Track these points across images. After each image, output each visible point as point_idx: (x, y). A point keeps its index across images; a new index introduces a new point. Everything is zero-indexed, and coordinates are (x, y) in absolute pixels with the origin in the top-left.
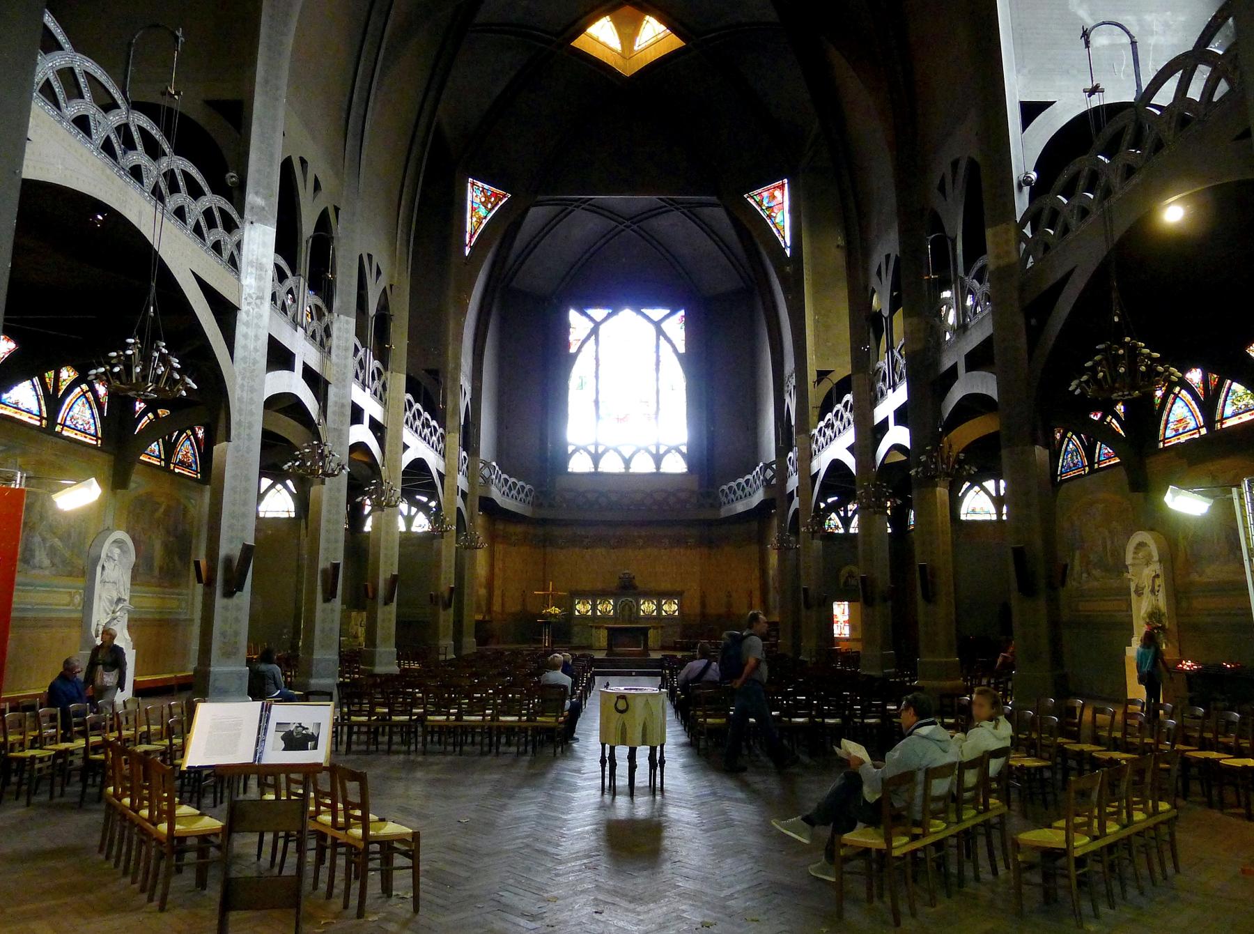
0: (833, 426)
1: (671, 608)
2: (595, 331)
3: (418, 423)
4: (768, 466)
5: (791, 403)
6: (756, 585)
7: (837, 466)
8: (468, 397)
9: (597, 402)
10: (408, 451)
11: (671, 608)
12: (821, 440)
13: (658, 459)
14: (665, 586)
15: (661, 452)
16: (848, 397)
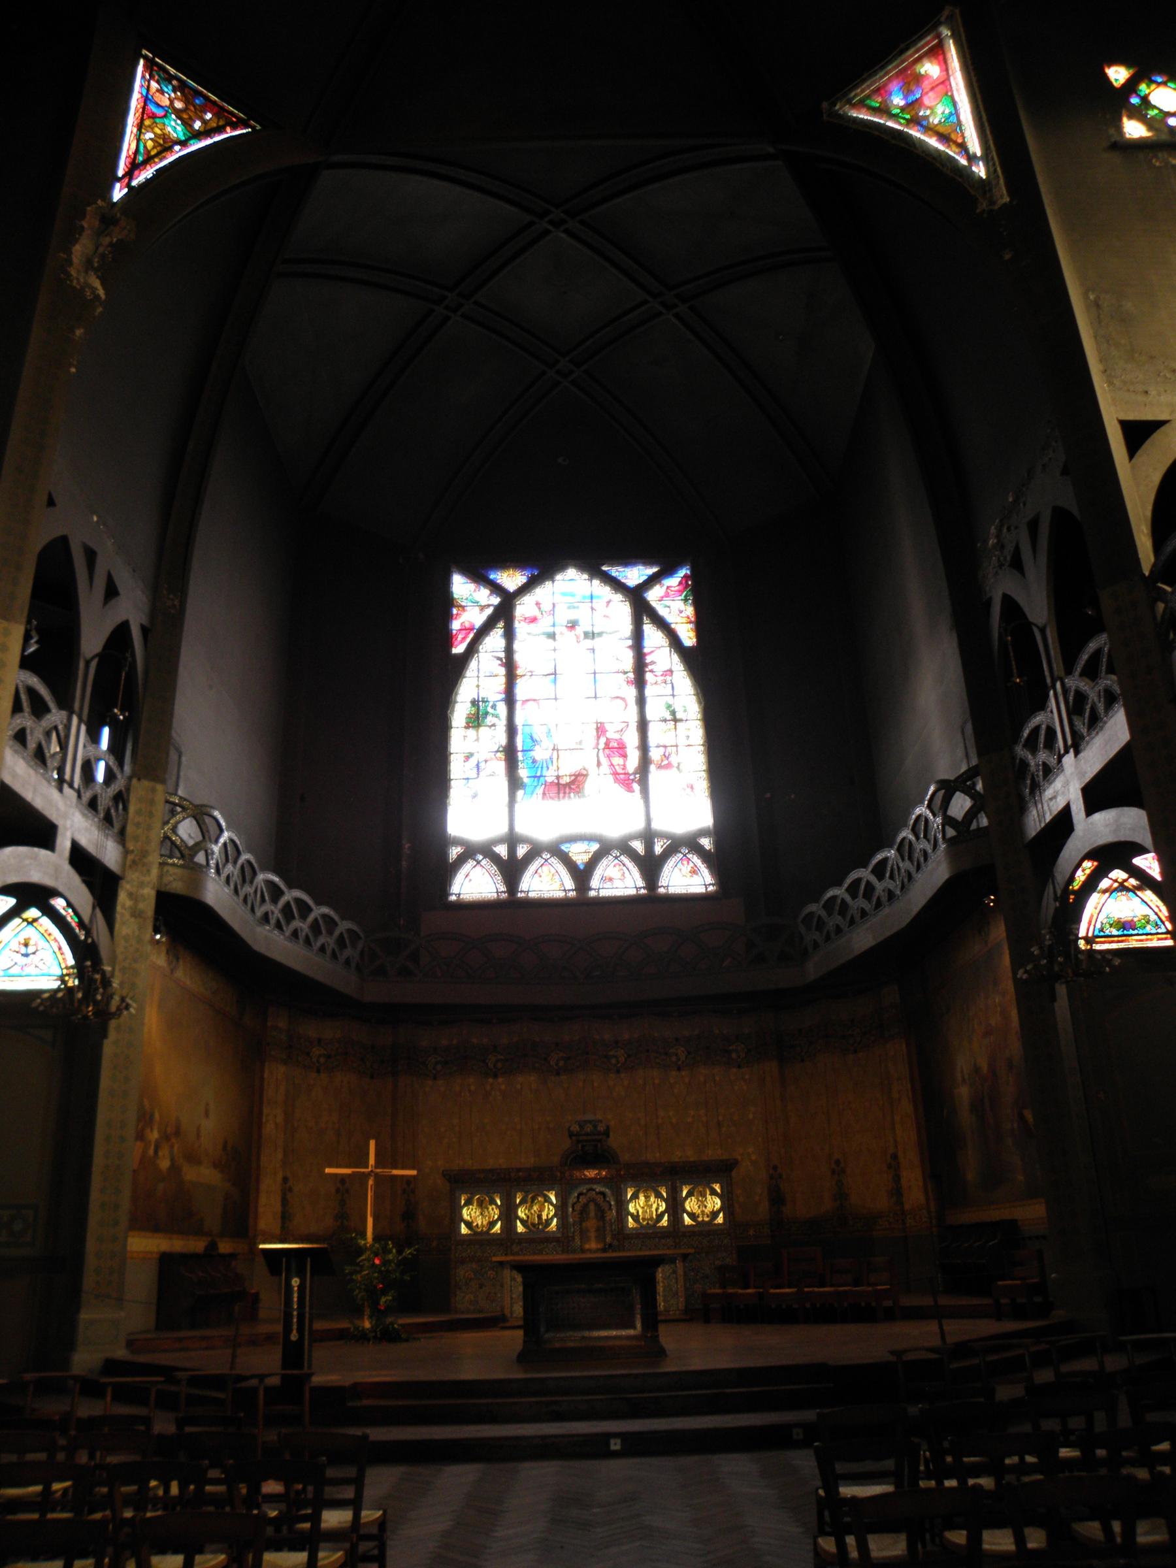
1: (704, 1205)
11: (704, 1205)
13: (650, 866)
14: (684, 1153)
15: (658, 850)
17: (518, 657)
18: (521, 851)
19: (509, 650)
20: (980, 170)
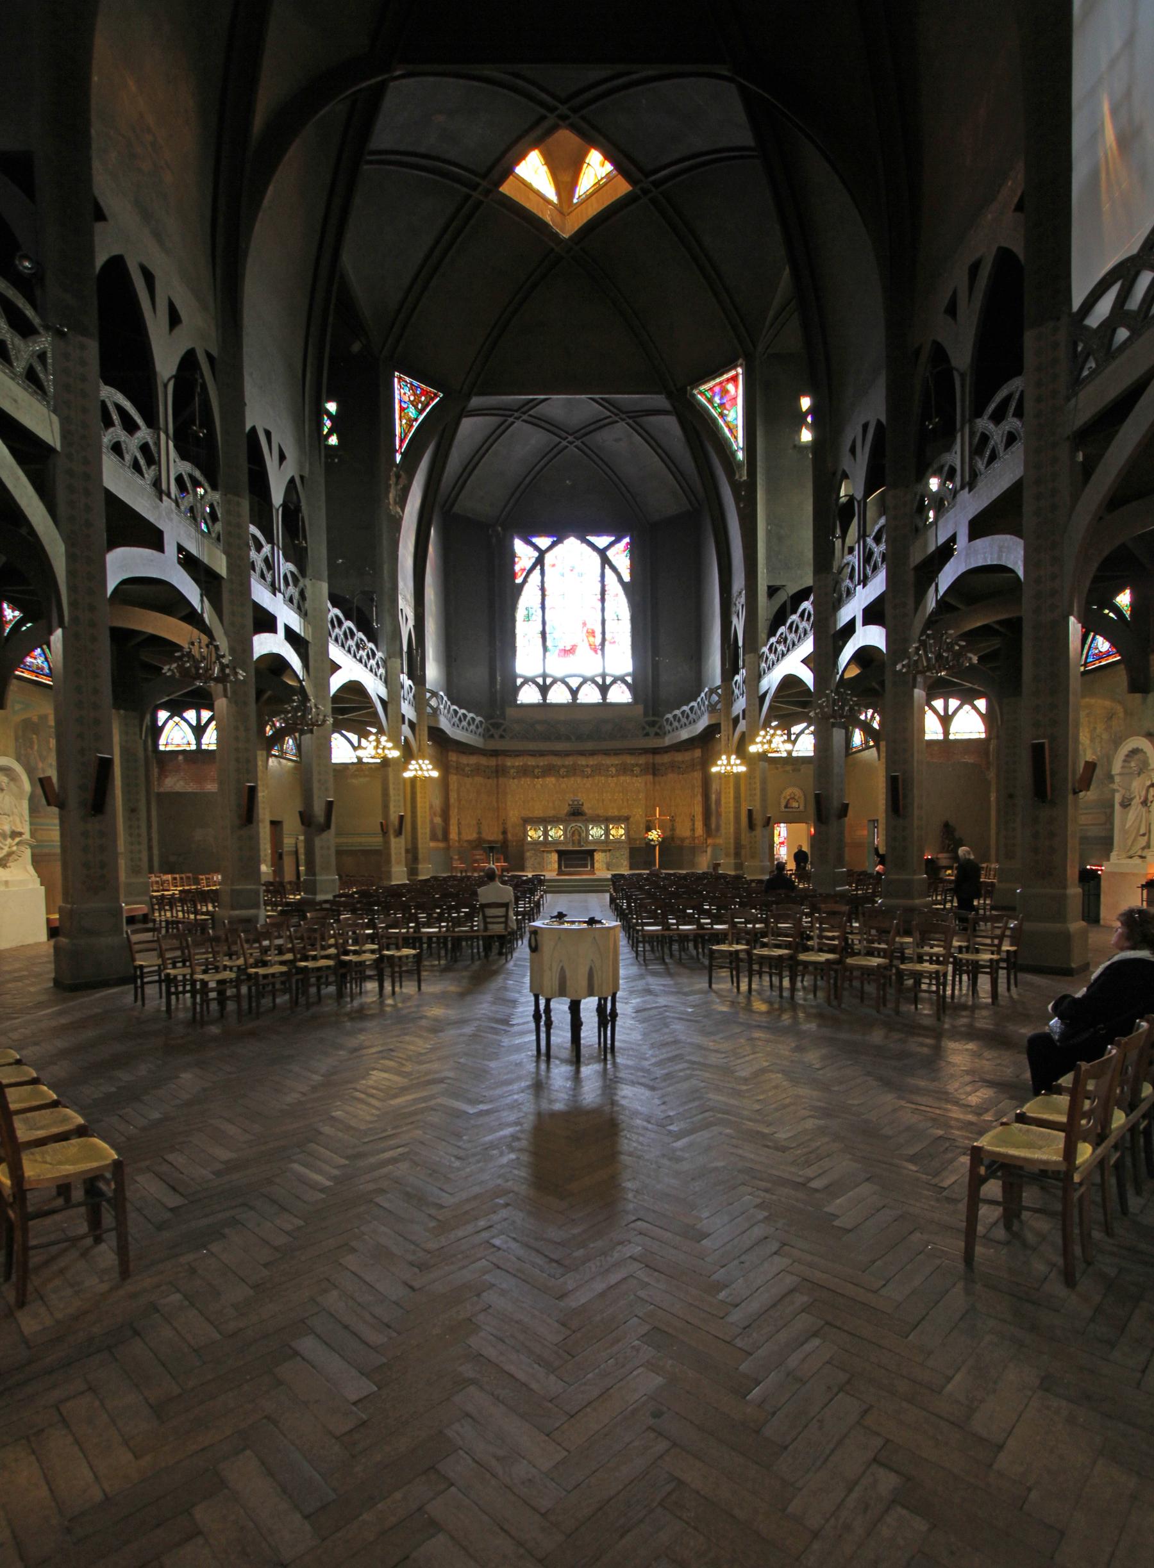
0: (786, 639)
1: (618, 832)
2: (540, 561)
3: (350, 642)
4: (712, 691)
5: (738, 624)
6: (698, 809)
7: (790, 682)
8: (411, 623)
9: (543, 634)
10: (339, 672)
11: (618, 832)
12: (772, 657)
13: (604, 689)
14: (613, 812)
16: (807, 605)
17: (546, 585)
18: (549, 681)
19: (543, 582)
20: (740, 455)
